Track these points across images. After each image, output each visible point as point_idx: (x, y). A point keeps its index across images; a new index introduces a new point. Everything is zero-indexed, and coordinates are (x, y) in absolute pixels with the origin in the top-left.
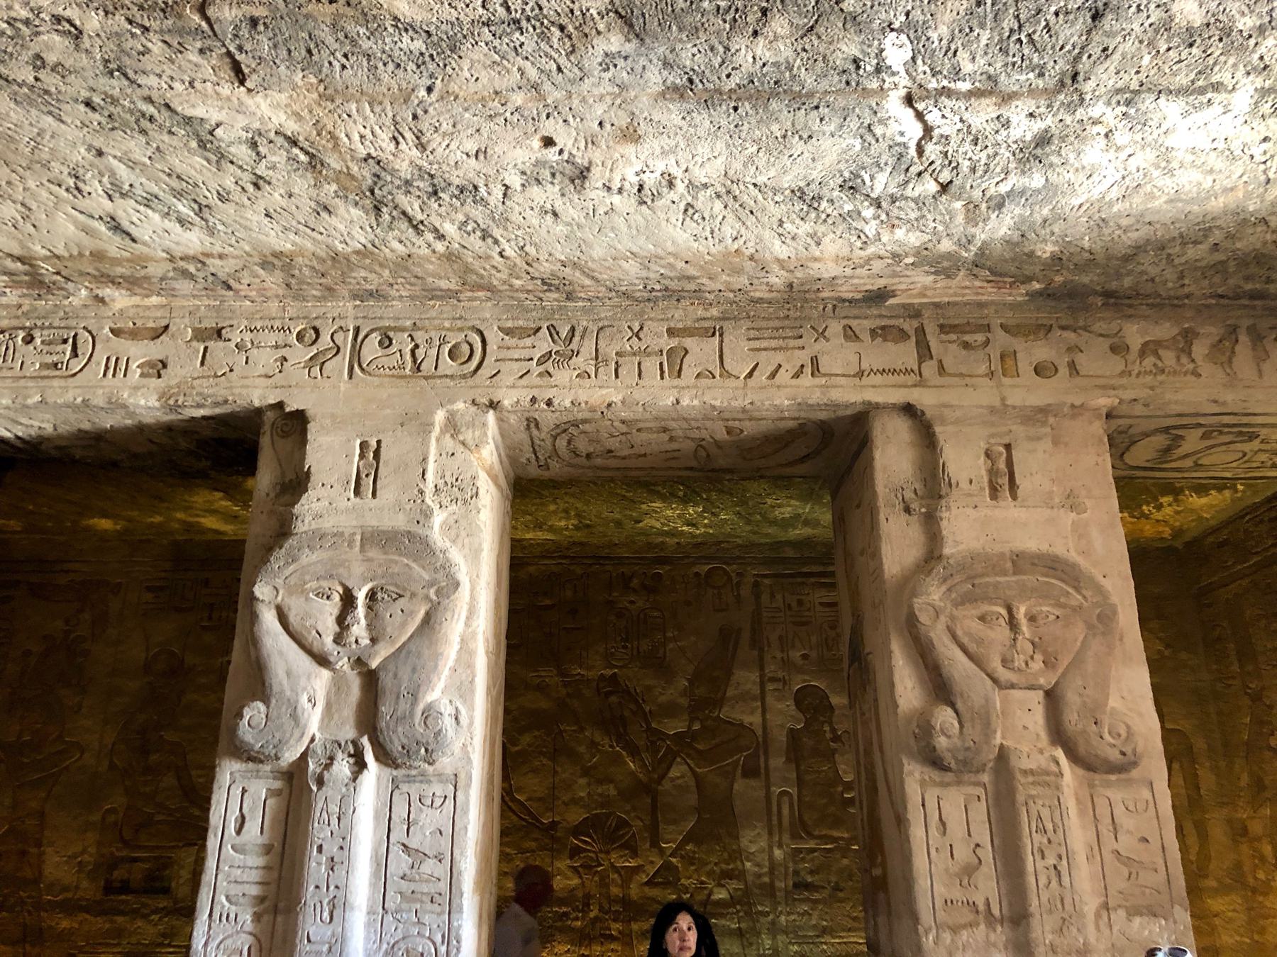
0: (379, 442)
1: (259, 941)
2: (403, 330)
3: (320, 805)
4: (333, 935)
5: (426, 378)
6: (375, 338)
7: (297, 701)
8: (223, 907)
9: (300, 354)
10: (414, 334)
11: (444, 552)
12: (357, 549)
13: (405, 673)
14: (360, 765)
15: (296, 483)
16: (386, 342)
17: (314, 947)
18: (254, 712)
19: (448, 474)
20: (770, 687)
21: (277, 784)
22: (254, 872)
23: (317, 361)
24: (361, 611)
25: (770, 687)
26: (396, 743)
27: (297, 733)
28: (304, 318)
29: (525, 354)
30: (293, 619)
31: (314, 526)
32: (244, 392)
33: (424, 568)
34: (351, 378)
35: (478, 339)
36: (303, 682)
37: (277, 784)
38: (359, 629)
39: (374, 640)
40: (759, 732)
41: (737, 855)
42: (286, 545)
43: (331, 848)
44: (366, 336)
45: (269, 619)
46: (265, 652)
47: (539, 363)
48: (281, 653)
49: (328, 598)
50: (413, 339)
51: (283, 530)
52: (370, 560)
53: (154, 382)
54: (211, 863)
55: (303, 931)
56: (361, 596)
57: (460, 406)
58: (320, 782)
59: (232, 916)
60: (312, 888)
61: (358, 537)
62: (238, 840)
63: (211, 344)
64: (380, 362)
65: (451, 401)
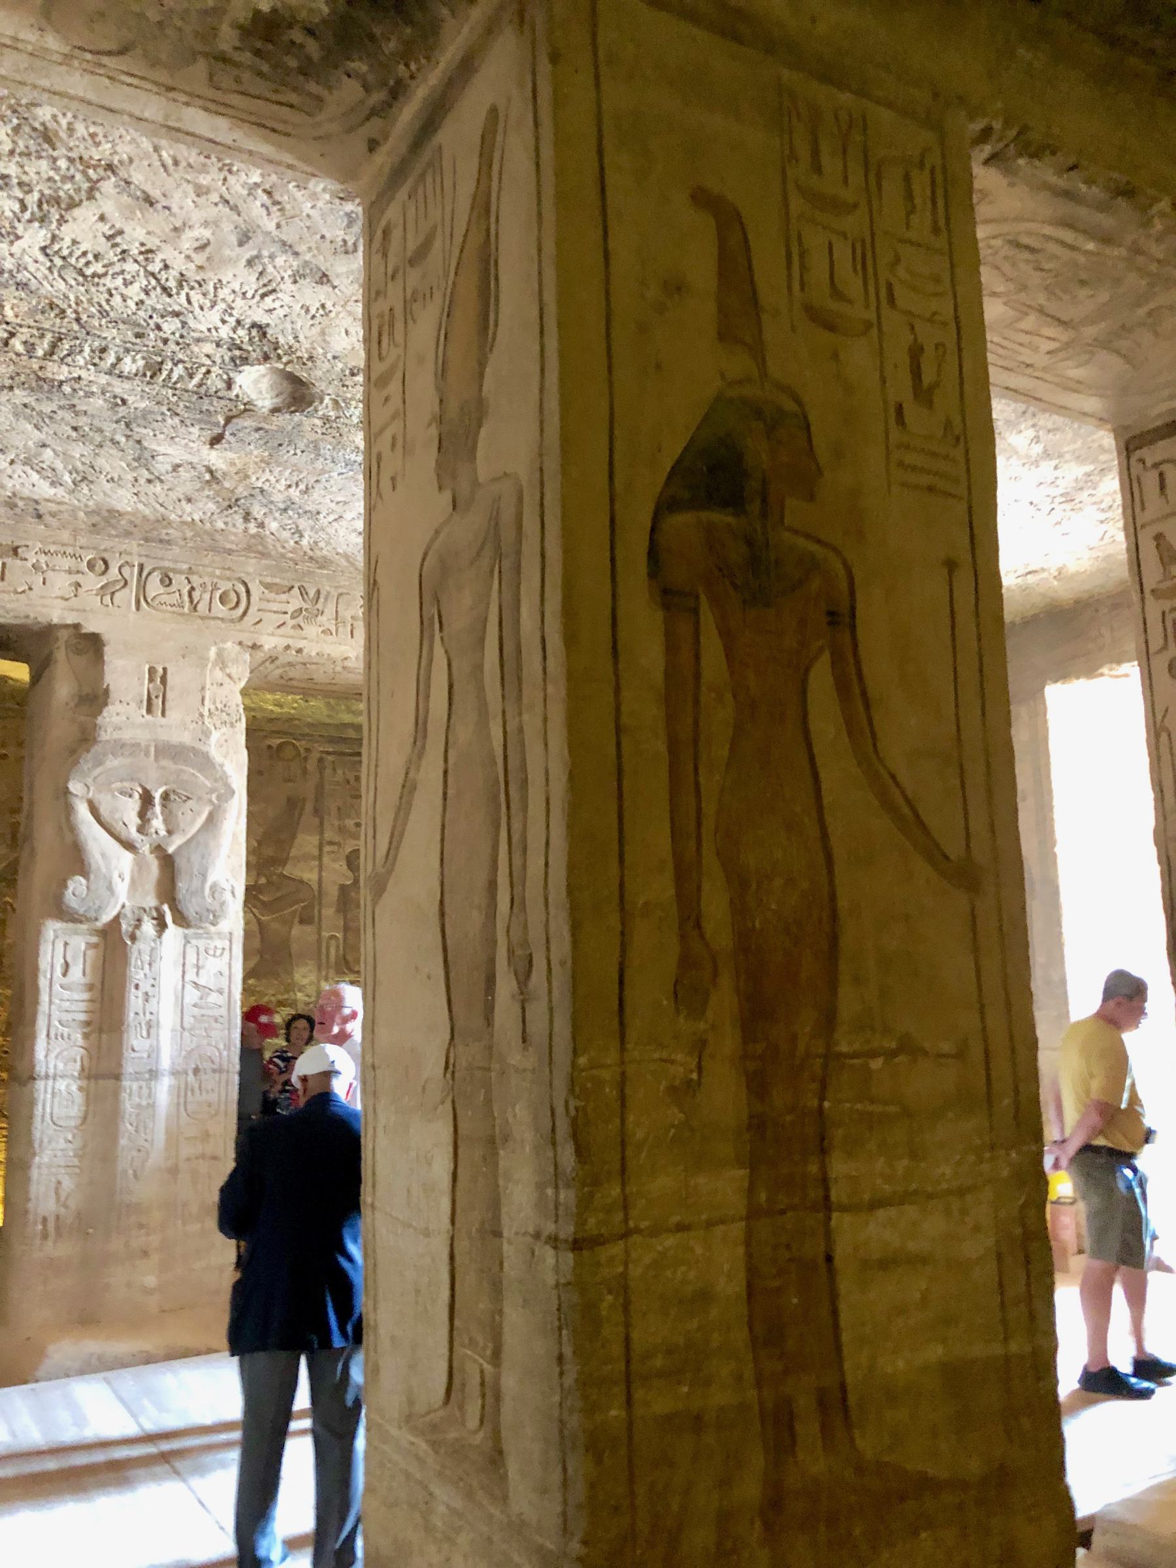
0: (165, 669)
2: (180, 572)
5: (202, 618)
6: (156, 577)
7: (111, 877)
9: (93, 582)
10: (190, 577)
11: (222, 766)
13: (195, 858)
14: (162, 926)
15: (95, 699)
16: (167, 581)
18: (76, 885)
19: (218, 702)
20: (327, 848)
21: (94, 939)
22: (81, 1004)
24: (158, 809)
25: (327, 848)
27: (113, 901)
28: (94, 548)
29: (283, 607)
30: (104, 811)
32: (44, 610)
33: (206, 777)
37: (94, 939)
38: (158, 823)
40: (315, 887)
41: (290, 987)
42: (93, 750)
43: (145, 986)
44: (149, 574)
45: (82, 811)
46: (82, 838)
47: (293, 617)
48: (95, 839)
51: (86, 738)
52: (163, 768)
54: (44, 997)
56: (157, 796)
57: (229, 645)
58: (133, 938)
59: (65, 1035)
60: (132, 1015)
61: (152, 749)
62: (65, 981)
65: (224, 641)
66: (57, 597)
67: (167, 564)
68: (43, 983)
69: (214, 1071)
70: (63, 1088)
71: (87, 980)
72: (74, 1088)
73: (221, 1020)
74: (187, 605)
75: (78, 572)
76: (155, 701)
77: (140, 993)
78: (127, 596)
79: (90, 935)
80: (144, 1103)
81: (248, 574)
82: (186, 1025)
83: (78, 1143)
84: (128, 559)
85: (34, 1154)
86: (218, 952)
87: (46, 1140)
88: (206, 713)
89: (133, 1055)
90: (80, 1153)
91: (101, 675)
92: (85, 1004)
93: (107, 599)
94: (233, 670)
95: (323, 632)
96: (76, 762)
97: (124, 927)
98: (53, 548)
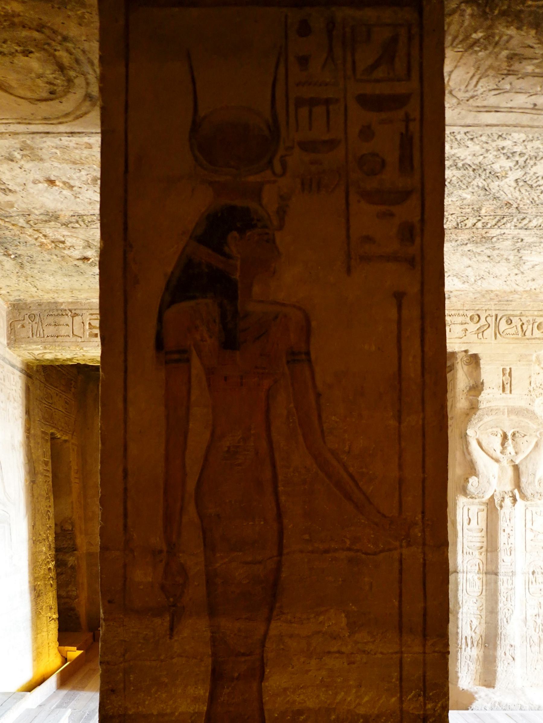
0: (510, 369)
2: (516, 316)
5: (528, 339)
9: (472, 327)
10: (522, 318)
14: (515, 500)
15: (477, 388)
16: (509, 322)
18: (473, 480)
19: (537, 382)
23: (480, 331)
28: (473, 310)
30: (484, 444)
34: (496, 338)
38: (510, 448)
39: (516, 453)
43: (508, 530)
44: (501, 319)
50: (521, 321)
51: (473, 408)
58: (501, 507)
59: (471, 553)
60: (502, 544)
61: (506, 411)
64: (508, 331)
66: (456, 338)
68: (459, 528)
71: (480, 527)
72: (476, 577)
75: (465, 323)
77: (505, 534)
78: (489, 333)
79: (480, 505)
80: (510, 587)
84: (490, 312)
85: (460, 607)
87: (464, 601)
88: (532, 390)
89: (504, 564)
91: (479, 375)
93: (480, 335)
96: (470, 421)
97: (496, 501)
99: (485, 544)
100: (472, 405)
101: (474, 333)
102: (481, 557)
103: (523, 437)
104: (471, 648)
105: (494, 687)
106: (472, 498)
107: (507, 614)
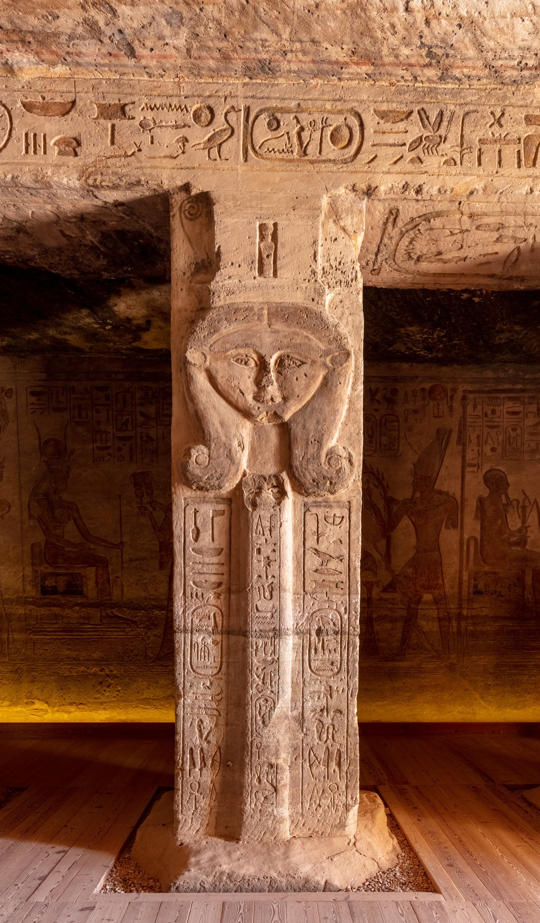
0: (275, 225)
1: (221, 610)
3: (256, 521)
4: (273, 607)
5: (312, 162)
6: (264, 119)
7: (231, 445)
8: (193, 588)
9: (199, 135)
10: (299, 116)
12: (265, 322)
13: (311, 425)
14: (282, 494)
16: (274, 124)
17: (262, 614)
18: (199, 454)
19: (332, 258)
23: (214, 143)
24: (273, 375)
26: (309, 477)
28: (199, 96)
30: (220, 380)
31: (228, 302)
32: (154, 172)
33: (320, 340)
34: (246, 160)
35: (354, 122)
36: (233, 430)
37: (221, 507)
38: (273, 390)
39: (285, 399)
43: (267, 551)
44: (256, 117)
45: (201, 380)
46: (201, 407)
47: (411, 150)
49: (246, 363)
50: (298, 122)
51: (202, 306)
52: (276, 332)
53: (71, 160)
54: (179, 560)
55: (253, 604)
57: (342, 191)
58: (254, 505)
59: (200, 594)
60: (255, 577)
61: (266, 312)
63: (116, 122)
64: (273, 144)
65: (336, 186)
67: (273, 104)
69: (336, 633)
70: (200, 640)
72: (209, 641)
73: (341, 585)
74: (296, 149)
75: (184, 126)
76: (266, 263)
79: (217, 503)
81: (361, 102)
82: (308, 589)
83: (215, 690)
86: (338, 521)
87: (188, 685)
90: (218, 698)
92: (216, 567)
94: (347, 221)
95: (446, 162)
97: (246, 494)
98: (158, 102)
99: (225, 577)
100: (200, 302)
101: (202, 146)
102: (219, 604)
103: (299, 366)
104: (201, 770)
105: (238, 840)
106: (200, 488)
107: (264, 708)
